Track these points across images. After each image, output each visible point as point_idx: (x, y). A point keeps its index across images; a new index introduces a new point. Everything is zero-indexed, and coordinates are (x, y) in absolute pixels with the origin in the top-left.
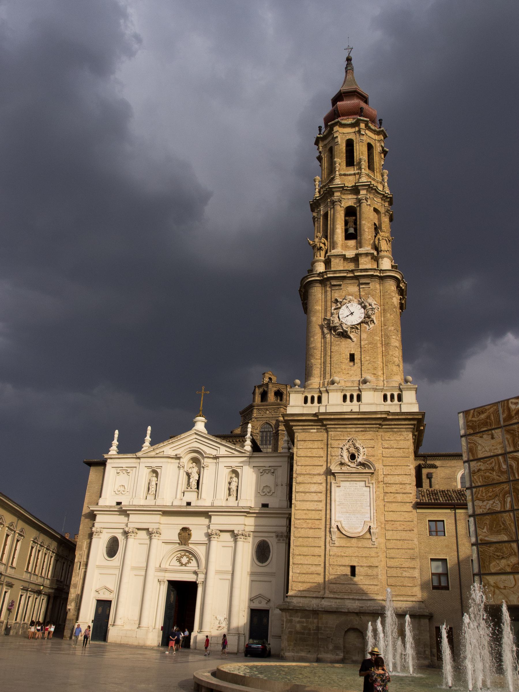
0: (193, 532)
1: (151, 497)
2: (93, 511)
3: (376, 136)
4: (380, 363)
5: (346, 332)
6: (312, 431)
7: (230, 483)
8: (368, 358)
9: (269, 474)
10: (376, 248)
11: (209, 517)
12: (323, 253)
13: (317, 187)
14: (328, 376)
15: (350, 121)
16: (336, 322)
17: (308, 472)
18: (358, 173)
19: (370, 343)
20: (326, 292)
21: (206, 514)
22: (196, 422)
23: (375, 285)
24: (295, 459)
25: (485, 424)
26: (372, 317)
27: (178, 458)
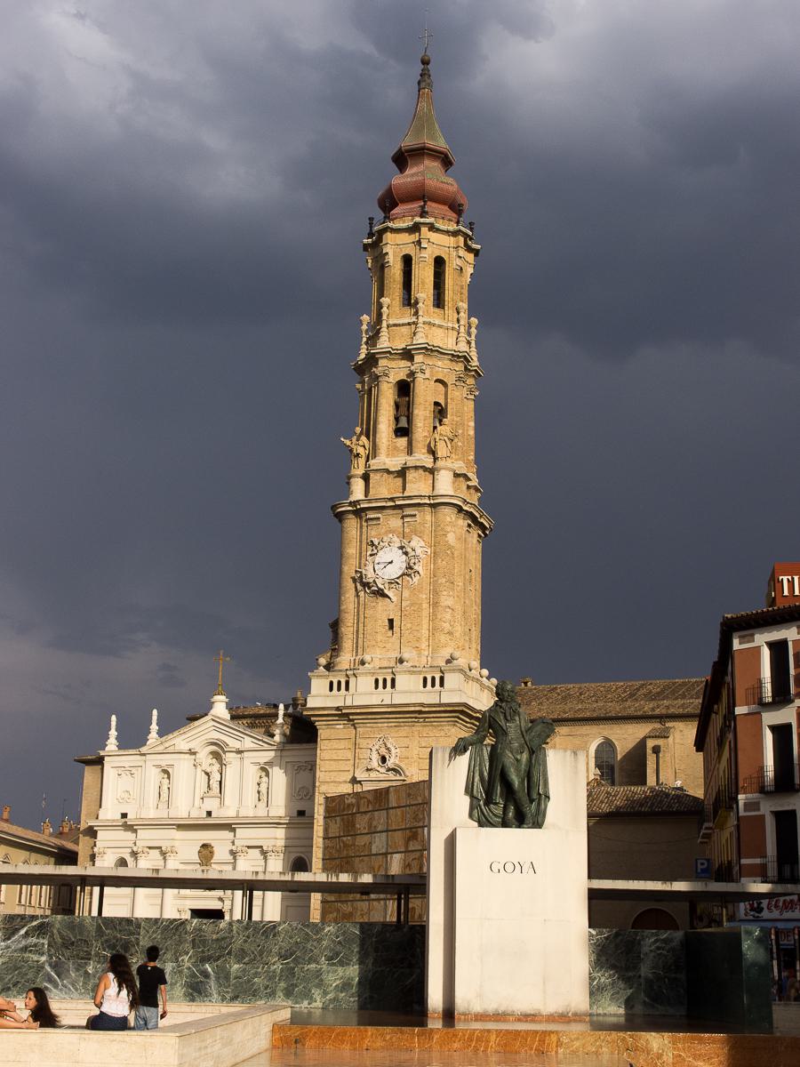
0: (215, 849)
1: (163, 806)
2: (91, 827)
3: (452, 238)
4: (425, 632)
5: (382, 590)
6: (338, 726)
7: (259, 784)
8: (409, 626)
9: (307, 771)
10: (432, 452)
11: (234, 830)
12: (362, 461)
13: (364, 335)
14: (360, 650)
15: (407, 223)
16: (369, 576)
17: (332, 780)
18: (414, 323)
19: (412, 605)
20: (361, 527)
21: (229, 827)
22: (213, 702)
23: (426, 516)
24: (318, 763)
25: (334, 811)
26: (416, 567)
27: (192, 753)
